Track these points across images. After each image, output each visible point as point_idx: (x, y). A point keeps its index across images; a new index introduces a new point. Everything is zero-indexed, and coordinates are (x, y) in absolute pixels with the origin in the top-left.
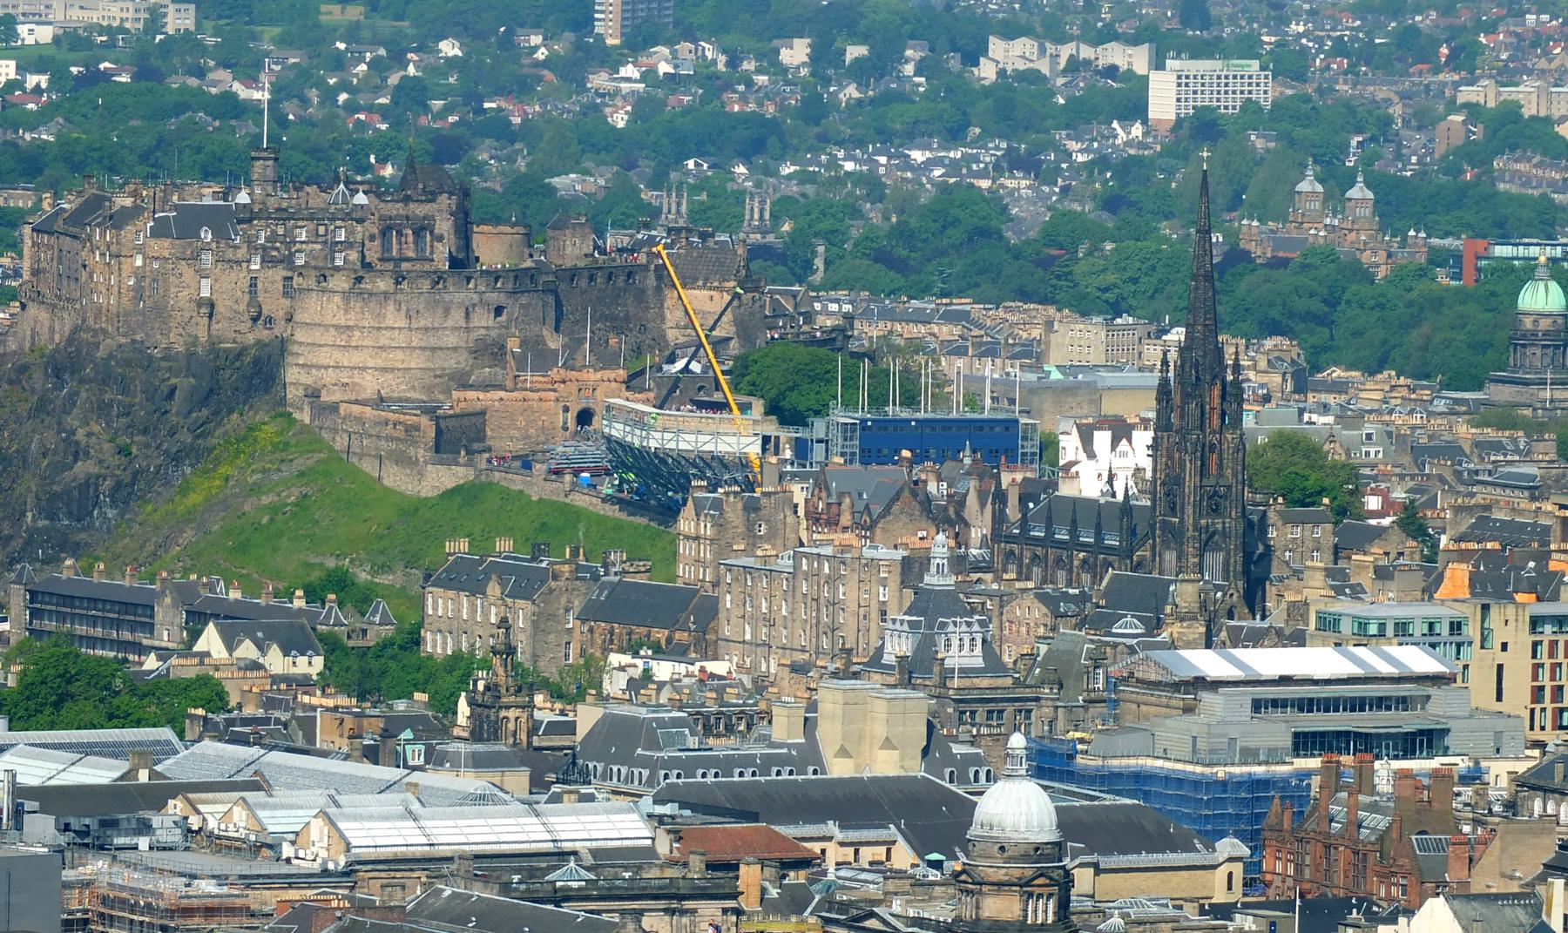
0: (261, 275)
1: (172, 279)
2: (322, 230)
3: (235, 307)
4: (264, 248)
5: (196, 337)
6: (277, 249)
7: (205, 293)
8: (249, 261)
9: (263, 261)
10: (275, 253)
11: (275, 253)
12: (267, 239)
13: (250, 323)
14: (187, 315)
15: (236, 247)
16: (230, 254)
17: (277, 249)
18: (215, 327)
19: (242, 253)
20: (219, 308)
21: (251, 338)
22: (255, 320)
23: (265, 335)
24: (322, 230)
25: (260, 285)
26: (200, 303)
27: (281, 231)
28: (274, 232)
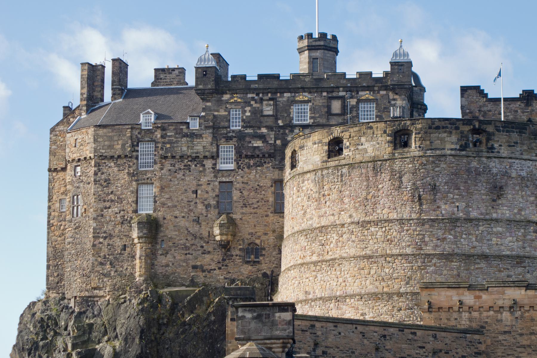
2: (336, 106)
3: (194, 229)
4: (241, 136)
6: (262, 137)
8: (215, 157)
9: (239, 155)
10: (258, 143)
11: (258, 143)
12: (247, 124)
15: (193, 135)
17: (262, 137)
20: (168, 231)
25: (236, 195)
27: (268, 110)
28: (257, 113)
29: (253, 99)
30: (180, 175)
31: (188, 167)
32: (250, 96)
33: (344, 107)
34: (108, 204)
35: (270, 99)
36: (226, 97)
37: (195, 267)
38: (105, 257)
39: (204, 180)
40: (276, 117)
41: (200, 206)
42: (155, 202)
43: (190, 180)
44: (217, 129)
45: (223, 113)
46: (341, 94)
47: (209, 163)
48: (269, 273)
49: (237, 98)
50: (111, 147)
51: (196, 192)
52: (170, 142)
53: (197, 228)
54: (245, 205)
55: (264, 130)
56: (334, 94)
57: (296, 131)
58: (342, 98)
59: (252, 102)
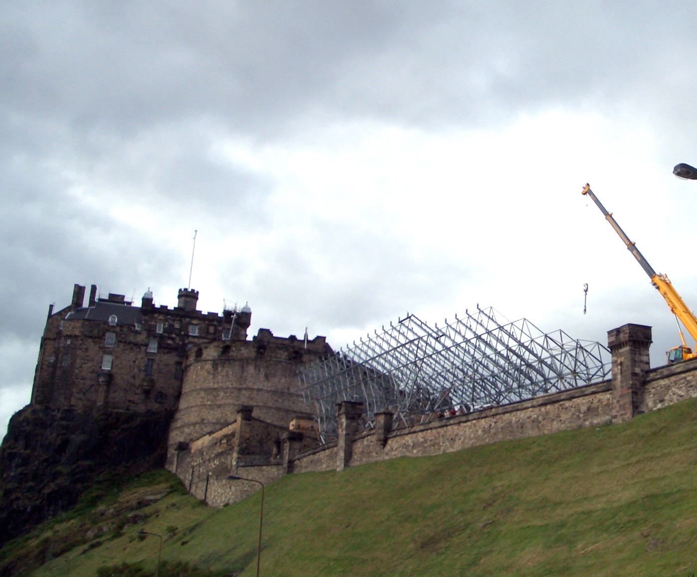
0: (157, 358)
1: (79, 352)
2: (212, 329)
4: (161, 337)
5: (95, 402)
6: (173, 339)
7: (106, 367)
8: (146, 345)
9: (160, 347)
10: (170, 342)
11: (170, 342)
12: (165, 330)
13: (142, 397)
14: (88, 383)
15: (137, 333)
16: (131, 338)
17: (173, 339)
18: (112, 395)
19: (141, 338)
20: (118, 381)
21: (142, 409)
22: (147, 393)
23: (155, 406)
24: (212, 329)
25: (155, 367)
26: (100, 373)
27: (177, 326)
28: (171, 326)
29: (170, 319)
30: (127, 352)
31: (132, 349)
32: (169, 317)
33: (216, 330)
34: (86, 362)
35: (179, 320)
36: (156, 315)
37: (130, 401)
38: (80, 390)
39: (139, 356)
40: (180, 330)
41: (136, 370)
42: (112, 364)
43: (131, 356)
44: (151, 332)
45: (153, 323)
46: (215, 323)
47: (143, 348)
48: (168, 409)
49: (161, 317)
50: (91, 332)
51: (134, 362)
52: (125, 334)
53: (133, 380)
54: (160, 373)
55: (174, 336)
56: (212, 323)
57: (190, 338)
58: (215, 325)
59: (169, 321)
